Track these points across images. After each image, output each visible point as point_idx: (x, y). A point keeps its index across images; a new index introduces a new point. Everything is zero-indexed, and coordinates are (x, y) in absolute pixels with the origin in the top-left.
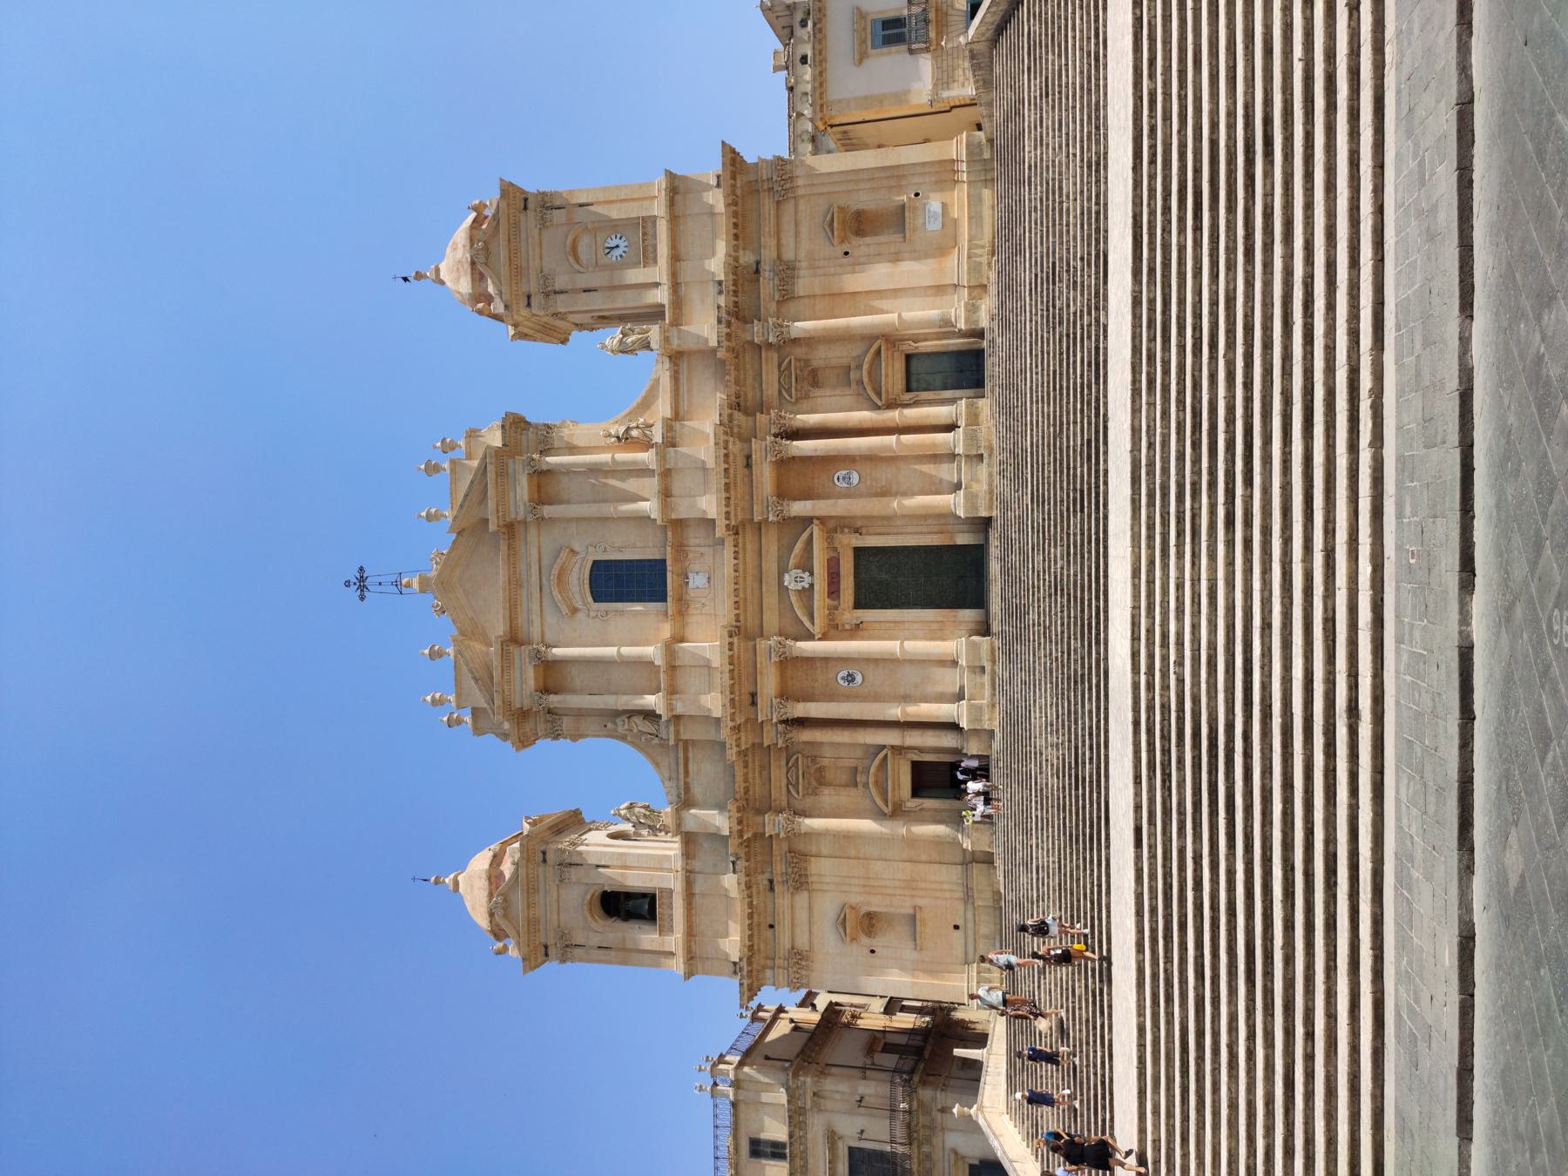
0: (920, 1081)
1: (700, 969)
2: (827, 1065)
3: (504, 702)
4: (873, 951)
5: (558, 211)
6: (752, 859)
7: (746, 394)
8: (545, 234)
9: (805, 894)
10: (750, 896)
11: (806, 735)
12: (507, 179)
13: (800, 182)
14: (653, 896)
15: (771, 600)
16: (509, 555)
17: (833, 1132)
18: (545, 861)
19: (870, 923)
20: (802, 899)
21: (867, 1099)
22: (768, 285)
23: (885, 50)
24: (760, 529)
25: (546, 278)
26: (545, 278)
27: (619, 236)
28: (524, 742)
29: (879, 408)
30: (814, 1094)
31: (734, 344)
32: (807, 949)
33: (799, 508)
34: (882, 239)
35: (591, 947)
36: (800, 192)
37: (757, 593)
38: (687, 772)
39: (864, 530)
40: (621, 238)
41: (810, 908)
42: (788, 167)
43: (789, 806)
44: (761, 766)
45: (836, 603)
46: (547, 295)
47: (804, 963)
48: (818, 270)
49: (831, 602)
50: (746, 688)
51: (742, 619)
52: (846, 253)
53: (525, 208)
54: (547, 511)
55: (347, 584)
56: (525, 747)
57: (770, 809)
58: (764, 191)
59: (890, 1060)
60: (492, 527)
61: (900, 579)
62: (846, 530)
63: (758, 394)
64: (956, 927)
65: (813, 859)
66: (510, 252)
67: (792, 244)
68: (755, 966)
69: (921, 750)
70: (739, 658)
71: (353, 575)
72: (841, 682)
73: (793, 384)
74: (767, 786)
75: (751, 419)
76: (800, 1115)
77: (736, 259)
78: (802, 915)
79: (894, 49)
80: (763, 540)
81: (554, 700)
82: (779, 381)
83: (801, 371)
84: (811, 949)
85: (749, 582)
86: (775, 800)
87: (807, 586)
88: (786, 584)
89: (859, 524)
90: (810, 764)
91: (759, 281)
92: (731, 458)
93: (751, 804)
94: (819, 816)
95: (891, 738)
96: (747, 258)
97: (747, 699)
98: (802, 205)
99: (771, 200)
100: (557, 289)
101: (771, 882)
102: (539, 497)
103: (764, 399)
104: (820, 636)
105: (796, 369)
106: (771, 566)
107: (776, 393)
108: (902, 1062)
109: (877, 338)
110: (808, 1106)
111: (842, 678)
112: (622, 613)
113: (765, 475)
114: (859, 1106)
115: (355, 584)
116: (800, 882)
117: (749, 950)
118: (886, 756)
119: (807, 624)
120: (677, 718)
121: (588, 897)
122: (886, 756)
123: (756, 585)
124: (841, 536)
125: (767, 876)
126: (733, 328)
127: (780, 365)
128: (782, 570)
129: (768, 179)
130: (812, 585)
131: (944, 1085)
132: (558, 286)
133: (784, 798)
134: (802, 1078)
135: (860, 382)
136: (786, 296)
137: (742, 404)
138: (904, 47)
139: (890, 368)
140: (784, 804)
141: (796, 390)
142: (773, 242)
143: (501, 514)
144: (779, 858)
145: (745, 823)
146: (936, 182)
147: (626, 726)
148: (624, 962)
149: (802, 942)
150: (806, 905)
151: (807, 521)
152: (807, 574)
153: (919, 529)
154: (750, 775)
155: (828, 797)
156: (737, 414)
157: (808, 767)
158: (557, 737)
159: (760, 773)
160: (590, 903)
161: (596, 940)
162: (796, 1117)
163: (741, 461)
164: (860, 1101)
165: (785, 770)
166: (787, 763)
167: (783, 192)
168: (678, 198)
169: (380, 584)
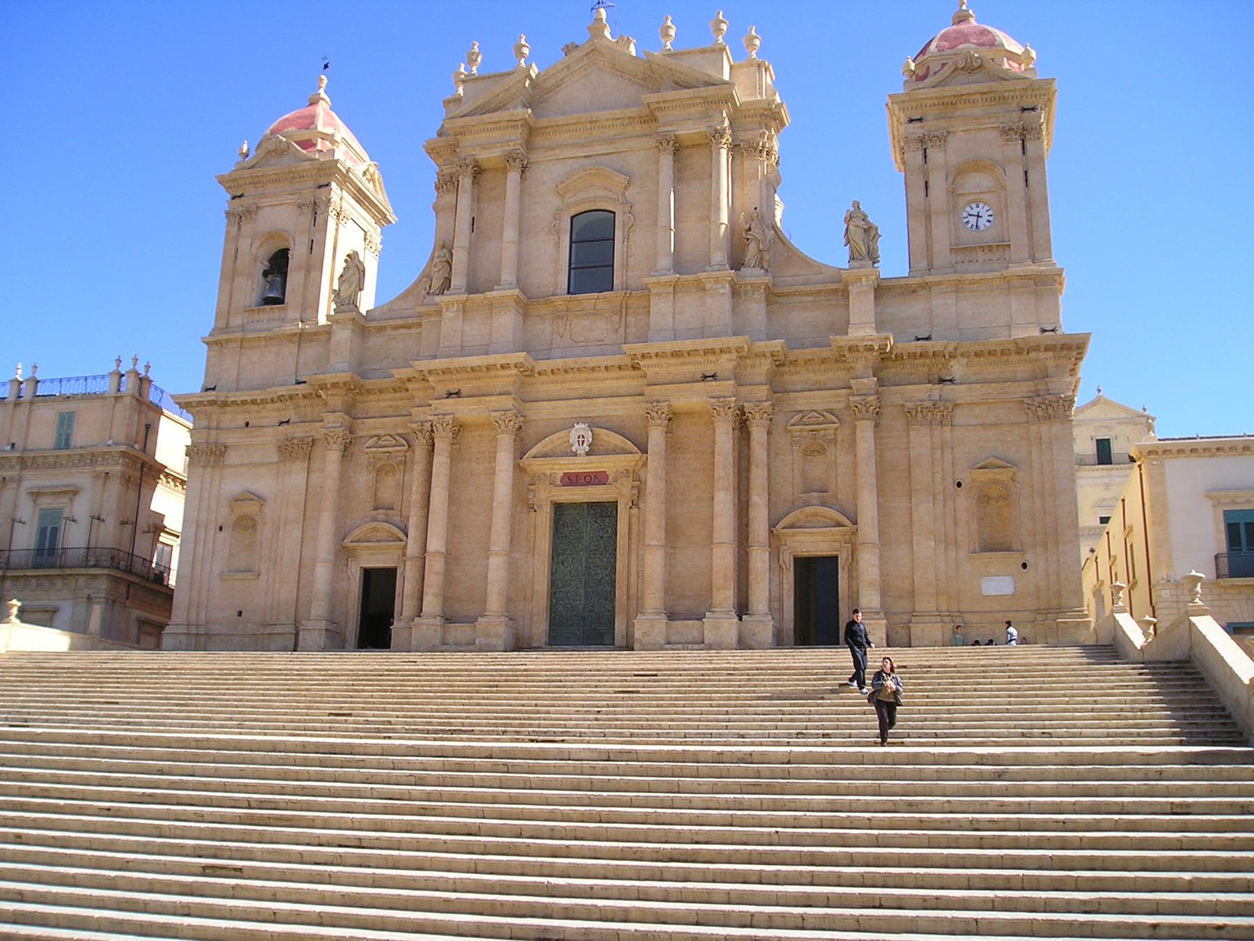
1: (212, 353)
3: (462, 127)
4: (221, 529)
5: (1019, 147)
6: (306, 402)
7: (797, 373)
8: (994, 135)
9: (275, 458)
11: (420, 453)
12: (1055, 86)
13: (1044, 428)
14: (283, 303)
15: (562, 409)
17: (75, 493)
18: (320, 187)
19: (247, 524)
21: (102, 525)
22: (921, 392)
23: (1222, 527)
24: (640, 395)
26: (942, 139)
27: (990, 218)
28: (432, 151)
29: (772, 525)
30: (107, 473)
31: (847, 356)
32: (226, 463)
33: (656, 437)
34: (974, 526)
35: (237, 243)
36: (1034, 428)
37: (572, 394)
38: (396, 328)
39: (635, 511)
40: (988, 221)
41: (263, 464)
42: (1060, 411)
44: (397, 407)
45: (559, 482)
46: (922, 141)
48: (940, 451)
49: (559, 477)
50: (466, 387)
51: (544, 378)
52: (959, 485)
53: (1024, 110)
54: (666, 160)
58: (1036, 386)
60: (652, 98)
63: (798, 387)
64: (240, 613)
66: (974, 94)
67: (974, 421)
68: (209, 409)
70: (496, 377)
73: (806, 427)
74: (378, 414)
75: (763, 379)
76: (91, 460)
77: (952, 356)
79: (1223, 536)
80: (627, 399)
81: (466, 182)
82: (812, 411)
83: (824, 436)
84: (224, 466)
85: (583, 385)
86: (363, 423)
88: (577, 426)
89: (641, 505)
90: (398, 459)
91: (929, 382)
92: (712, 358)
93: (358, 397)
95: (413, 548)
96: (957, 369)
97: (453, 387)
99: (1025, 395)
102: (688, 146)
103: (792, 394)
104: (521, 465)
105: (825, 429)
106: (602, 408)
107: (799, 408)
109: (855, 523)
110: (99, 469)
112: (558, 245)
113: (692, 398)
114: (93, 518)
117: (222, 402)
118: (402, 540)
119: (534, 451)
120: (439, 313)
122: (402, 540)
123: (581, 393)
124: (630, 486)
125: (294, 418)
126: (865, 354)
127: (831, 411)
128: (593, 424)
129: (1048, 390)
130: (575, 454)
131: (114, 601)
133: (365, 433)
134: (121, 461)
135: (807, 504)
136: (911, 415)
137: (786, 369)
138: (1223, 548)
139: (820, 538)
140: (360, 433)
141: (801, 431)
143: (662, 105)
144: (308, 429)
145: (335, 391)
146: (1037, 587)
147: (438, 260)
148: (223, 276)
149: (232, 458)
151: (644, 451)
153: (634, 573)
154: (388, 396)
155: (362, 479)
156: (766, 365)
157: (396, 457)
158: (437, 188)
159: (392, 407)
161: (244, 244)
162: (89, 458)
163: (709, 369)
164: (99, 519)
165: (392, 432)
166: (399, 435)
167: (1033, 408)
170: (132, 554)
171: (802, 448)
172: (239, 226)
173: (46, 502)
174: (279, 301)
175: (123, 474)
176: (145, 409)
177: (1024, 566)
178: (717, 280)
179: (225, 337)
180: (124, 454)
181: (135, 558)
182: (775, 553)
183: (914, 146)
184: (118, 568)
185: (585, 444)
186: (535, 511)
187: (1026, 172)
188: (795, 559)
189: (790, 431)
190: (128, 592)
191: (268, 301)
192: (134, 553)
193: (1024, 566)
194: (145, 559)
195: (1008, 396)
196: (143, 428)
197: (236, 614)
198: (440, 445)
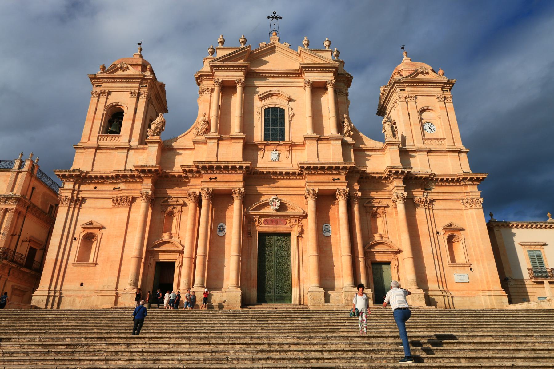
0: (4, 264)
2: (25, 217)
4: (75, 239)
10: (112, 177)
20: (109, 203)
23: (528, 257)
43: (156, 198)
46: (406, 98)
47: (74, 203)
51: (255, 175)
52: (438, 233)
55: (275, 13)
56: (197, 79)
57: (156, 188)
59: (23, 250)
61: (273, 258)
62: (300, 229)
64: (82, 284)
65: (128, 209)
69: (181, 267)
71: (278, 14)
72: (220, 225)
78: (100, 203)
94: (152, 213)
98: (458, 212)
100: (409, 103)
101: (119, 188)
105: (380, 207)
108: (20, 256)
111: (222, 226)
115: (275, 15)
116: (118, 202)
121: (122, 104)
140: (158, 195)
142: (441, 198)
150: (105, 206)
152: (277, 208)
160: (118, 105)
168: (457, 154)
169: (275, 24)
170: (15, 252)
171: (371, 214)
172: (99, 99)
174: (117, 132)
175: (16, 210)
176: (33, 179)
177: (471, 269)
180: (18, 200)
181: (16, 254)
183: (403, 99)
184: (6, 259)
185: (277, 206)
186: (251, 236)
189: (365, 207)
190: (9, 273)
191: (111, 133)
192: (16, 251)
193: (471, 269)
194: (22, 255)
195: (455, 197)
196: (30, 189)
197: (80, 284)
198: (204, 202)
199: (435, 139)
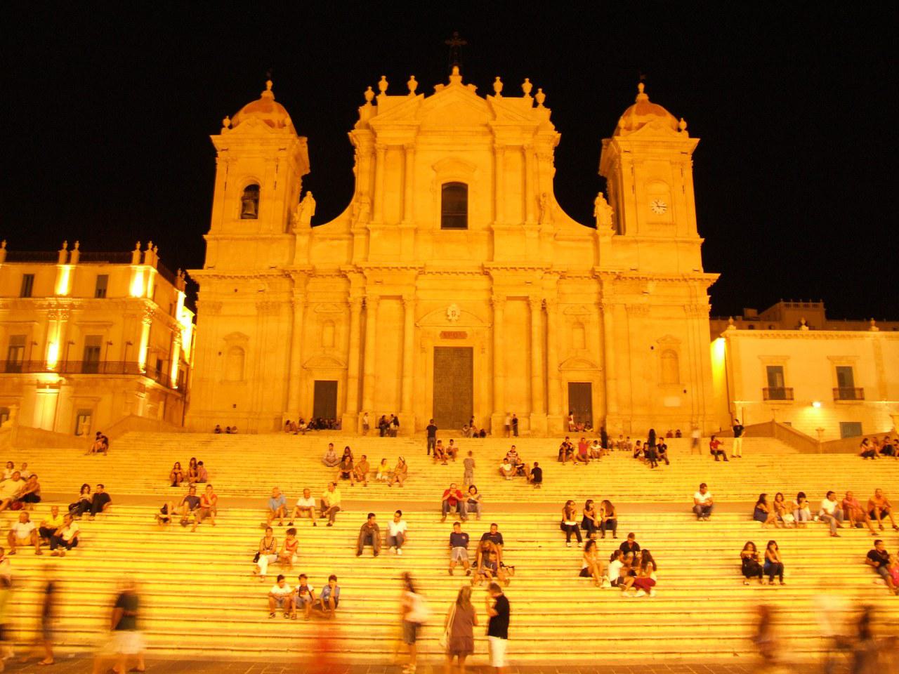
4: (220, 353)
16: (473, 132)
17: (111, 325)
20: (253, 311)
23: (766, 374)
25: (642, 162)
38: (333, 239)
52: (652, 348)
61: (451, 377)
64: (235, 406)
79: (766, 379)
87: (450, 318)
95: (354, 370)
116: (265, 309)
132: (637, 170)
149: (225, 310)
152: (456, 318)
173: (91, 332)
177: (685, 391)
178: (531, 230)
179: (221, 236)
182: (560, 380)
185: (456, 316)
187: (683, 187)
188: (569, 383)
197: (232, 405)
199: (662, 224)
